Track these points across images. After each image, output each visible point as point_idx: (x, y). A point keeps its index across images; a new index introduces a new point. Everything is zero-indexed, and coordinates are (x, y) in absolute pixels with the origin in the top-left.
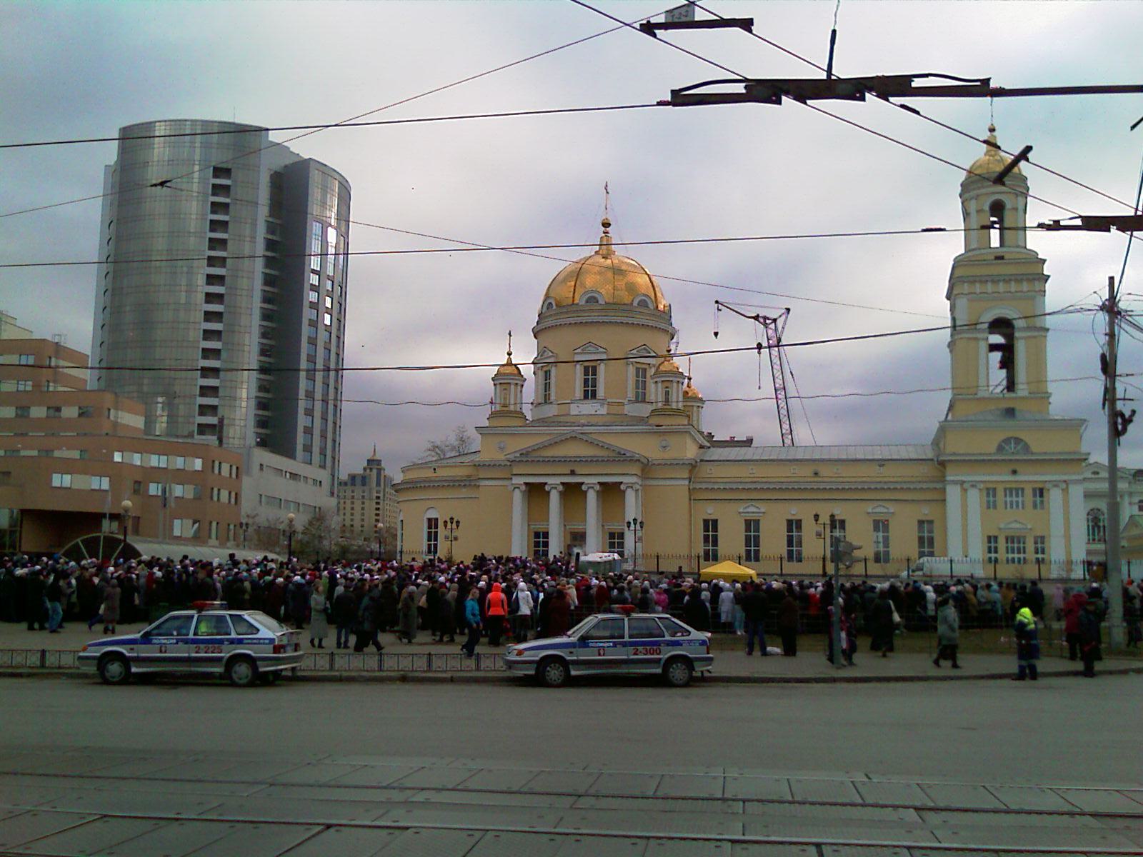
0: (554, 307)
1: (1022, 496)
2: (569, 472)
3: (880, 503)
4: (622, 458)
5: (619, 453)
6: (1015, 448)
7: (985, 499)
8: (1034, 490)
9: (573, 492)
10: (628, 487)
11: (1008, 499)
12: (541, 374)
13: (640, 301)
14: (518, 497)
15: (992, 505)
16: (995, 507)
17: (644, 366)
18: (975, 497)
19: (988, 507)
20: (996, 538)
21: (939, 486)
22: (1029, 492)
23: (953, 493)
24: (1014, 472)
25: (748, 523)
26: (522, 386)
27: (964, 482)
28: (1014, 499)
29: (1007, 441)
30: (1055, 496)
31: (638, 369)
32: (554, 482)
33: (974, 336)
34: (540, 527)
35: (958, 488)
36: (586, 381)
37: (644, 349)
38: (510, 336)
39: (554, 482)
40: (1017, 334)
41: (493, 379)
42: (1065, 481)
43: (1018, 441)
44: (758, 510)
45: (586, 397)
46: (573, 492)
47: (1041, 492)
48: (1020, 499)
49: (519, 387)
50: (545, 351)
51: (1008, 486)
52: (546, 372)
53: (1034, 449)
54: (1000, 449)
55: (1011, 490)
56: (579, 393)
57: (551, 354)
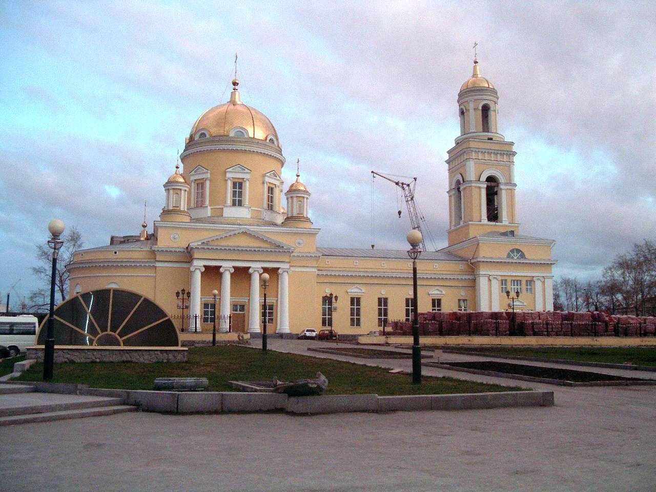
0: (208, 136)
1: (520, 286)
3: (438, 288)
4: (279, 249)
5: (279, 246)
8: (527, 281)
9: (241, 274)
10: (284, 271)
11: (513, 287)
13: (270, 139)
14: (198, 276)
17: (274, 186)
18: (496, 285)
21: (471, 277)
22: (524, 283)
23: (483, 283)
25: (352, 299)
29: (512, 251)
30: (538, 285)
32: (227, 267)
33: (478, 185)
34: (243, 300)
36: (240, 194)
37: (274, 174)
39: (227, 267)
40: (502, 187)
41: (165, 186)
42: (543, 277)
43: (518, 251)
44: (360, 291)
45: (234, 204)
46: (241, 274)
50: (199, 168)
51: (514, 279)
52: (198, 184)
53: (527, 256)
54: (509, 256)
55: (514, 281)
56: (229, 202)
57: (205, 170)
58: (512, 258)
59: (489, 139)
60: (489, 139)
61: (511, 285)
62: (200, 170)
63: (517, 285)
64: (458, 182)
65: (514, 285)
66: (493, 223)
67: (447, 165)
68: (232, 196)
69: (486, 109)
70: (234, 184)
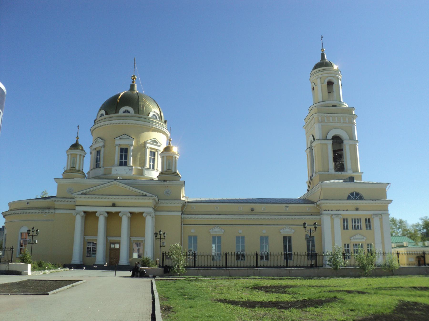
1: (360, 223)
2: (112, 205)
6: (356, 197)
7: (342, 224)
12: (94, 153)
15: (345, 227)
16: (347, 229)
17: (154, 151)
18: (338, 223)
19: (344, 229)
20: (348, 245)
22: (363, 221)
23: (326, 220)
24: (357, 209)
26: (84, 157)
27: (332, 215)
28: (357, 224)
31: (151, 152)
35: (329, 217)
37: (155, 140)
38: (79, 129)
45: (121, 164)
47: (368, 220)
48: (359, 224)
49: (82, 157)
58: (352, 199)
59: (333, 106)
60: (333, 106)
61: (353, 223)
62: (98, 141)
63: (358, 223)
64: (312, 143)
65: (355, 223)
66: (339, 173)
67: (305, 130)
68: (119, 159)
69: (330, 84)
70: (122, 150)
